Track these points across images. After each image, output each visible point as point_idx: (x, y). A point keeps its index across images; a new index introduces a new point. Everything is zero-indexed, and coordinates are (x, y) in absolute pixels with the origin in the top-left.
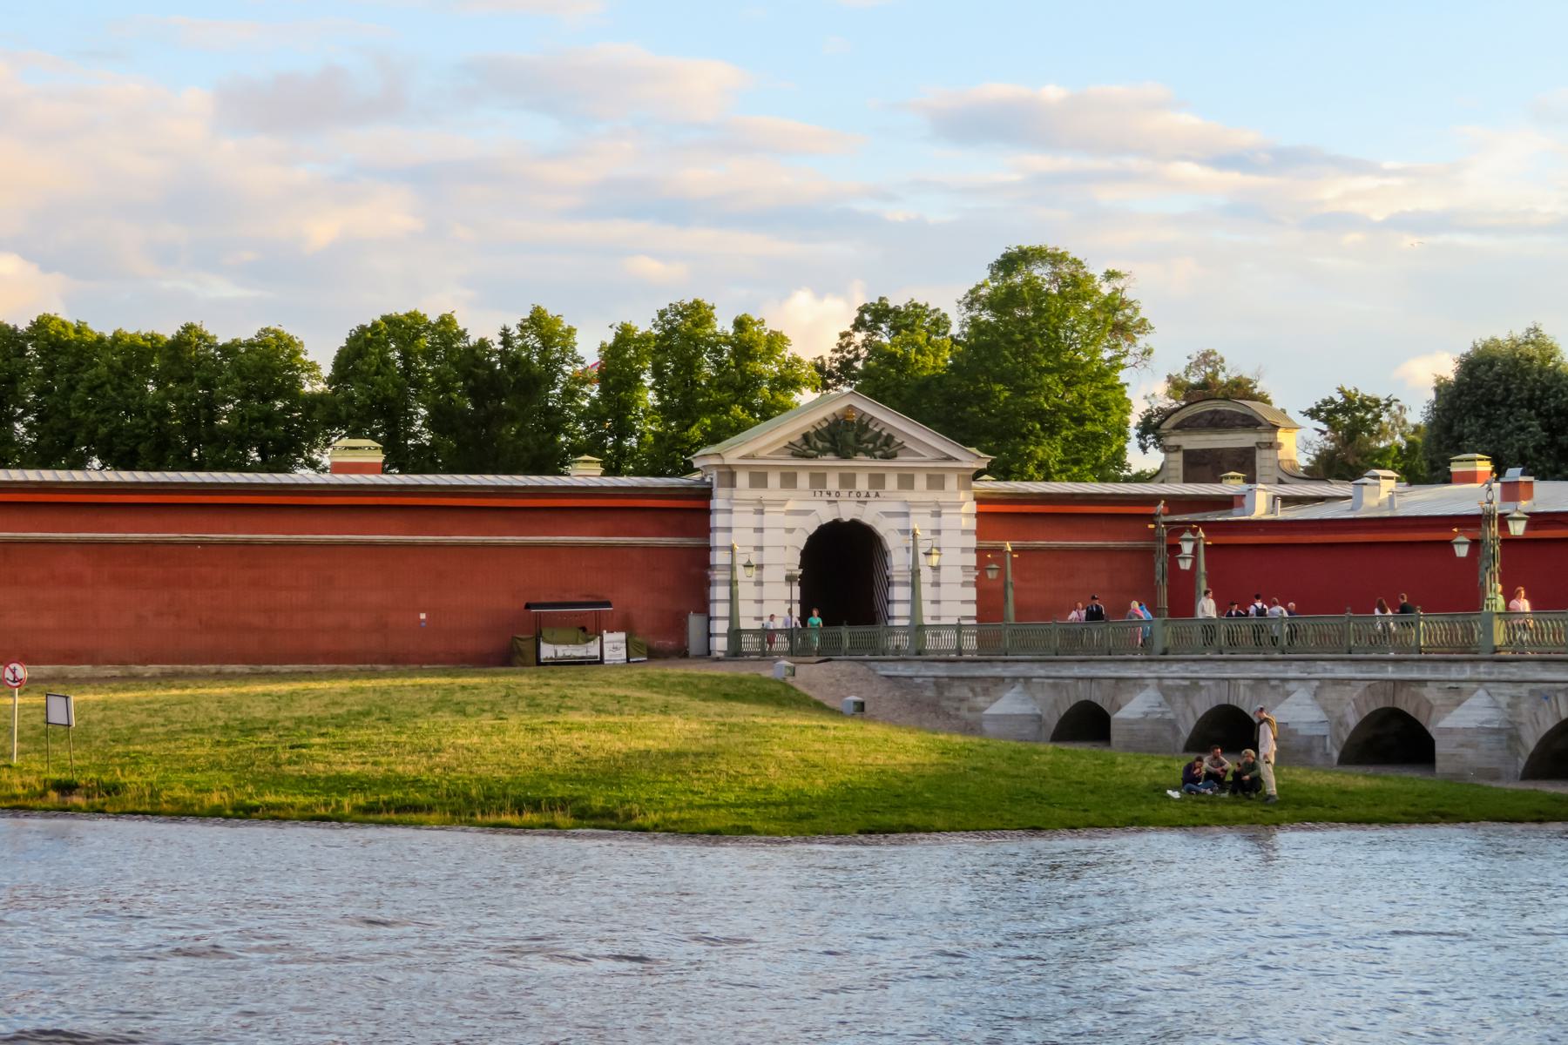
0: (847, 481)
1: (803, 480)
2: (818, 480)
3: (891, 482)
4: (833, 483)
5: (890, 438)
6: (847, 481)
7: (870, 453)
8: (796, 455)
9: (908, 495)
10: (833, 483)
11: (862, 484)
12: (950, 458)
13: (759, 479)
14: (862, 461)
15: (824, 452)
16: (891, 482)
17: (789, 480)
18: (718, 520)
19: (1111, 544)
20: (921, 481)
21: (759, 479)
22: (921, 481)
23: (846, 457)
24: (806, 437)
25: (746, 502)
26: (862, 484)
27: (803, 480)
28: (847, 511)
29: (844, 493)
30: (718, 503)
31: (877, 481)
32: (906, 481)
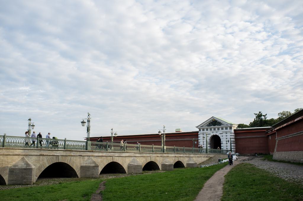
0: (215, 129)
1: (209, 130)
2: (211, 129)
3: (220, 129)
4: (213, 130)
5: (220, 123)
6: (215, 129)
7: (218, 125)
8: (208, 126)
9: (222, 131)
10: (213, 130)
11: (216, 129)
12: (227, 125)
13: (203, 130)
14: (216, 126)
15: (211, 125)
16: (220, 129)
17: (207, 130)
18: (199, 136)
19: (258, 136)
20: (224, 129)
21: (203, 130)
22: (224, 129)
23: (214, 126)
24: (209, 123)
25: (201, 133)
26: (216, 129)
27: (209, 130)
28: (215, 134)
29: (214, 131)
30: (199, 134)
31: (218, 129)
32: (222, 129)
